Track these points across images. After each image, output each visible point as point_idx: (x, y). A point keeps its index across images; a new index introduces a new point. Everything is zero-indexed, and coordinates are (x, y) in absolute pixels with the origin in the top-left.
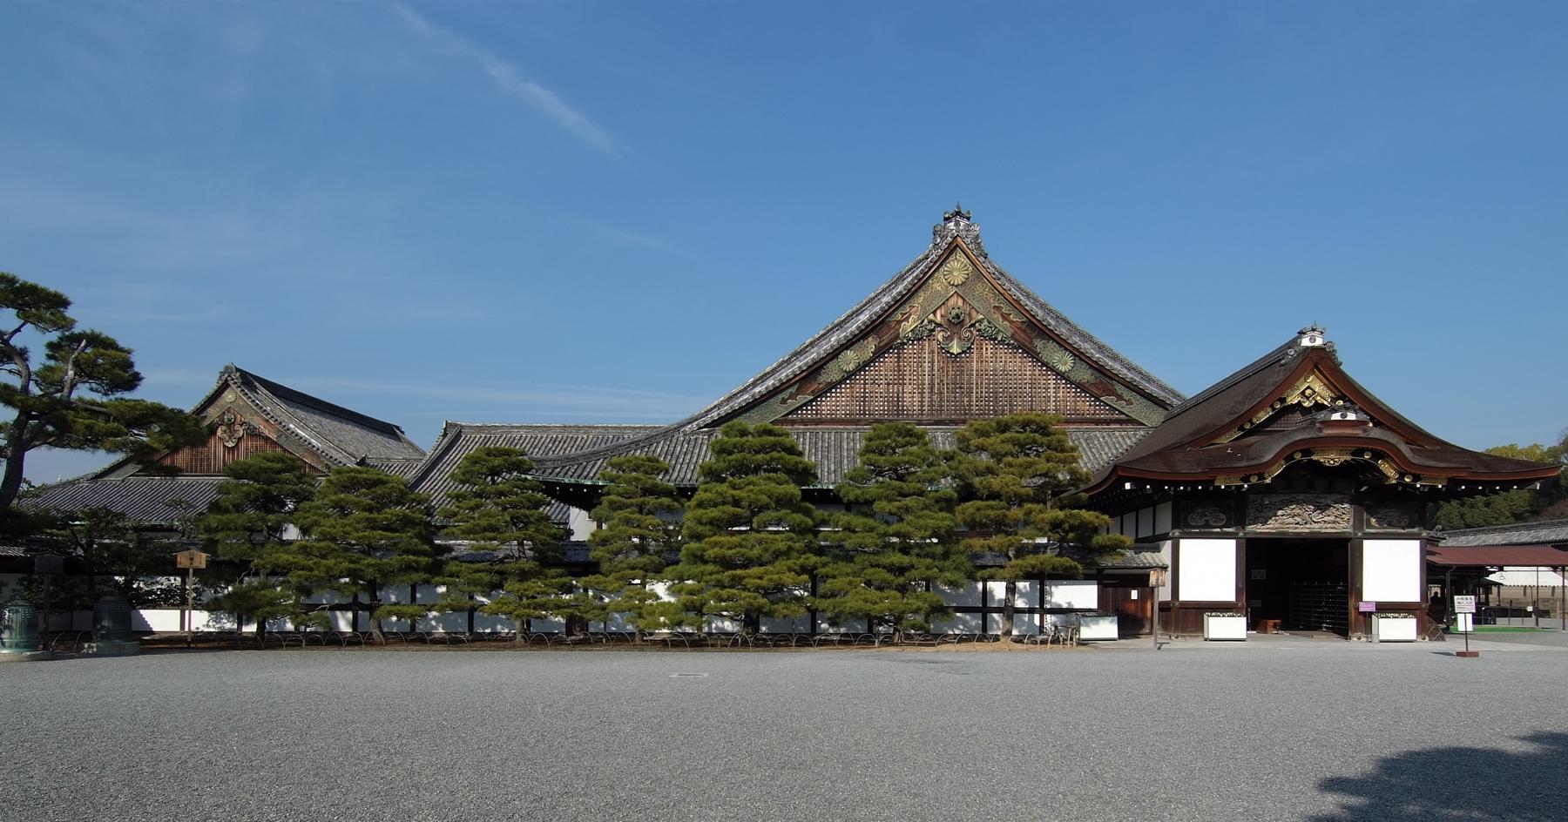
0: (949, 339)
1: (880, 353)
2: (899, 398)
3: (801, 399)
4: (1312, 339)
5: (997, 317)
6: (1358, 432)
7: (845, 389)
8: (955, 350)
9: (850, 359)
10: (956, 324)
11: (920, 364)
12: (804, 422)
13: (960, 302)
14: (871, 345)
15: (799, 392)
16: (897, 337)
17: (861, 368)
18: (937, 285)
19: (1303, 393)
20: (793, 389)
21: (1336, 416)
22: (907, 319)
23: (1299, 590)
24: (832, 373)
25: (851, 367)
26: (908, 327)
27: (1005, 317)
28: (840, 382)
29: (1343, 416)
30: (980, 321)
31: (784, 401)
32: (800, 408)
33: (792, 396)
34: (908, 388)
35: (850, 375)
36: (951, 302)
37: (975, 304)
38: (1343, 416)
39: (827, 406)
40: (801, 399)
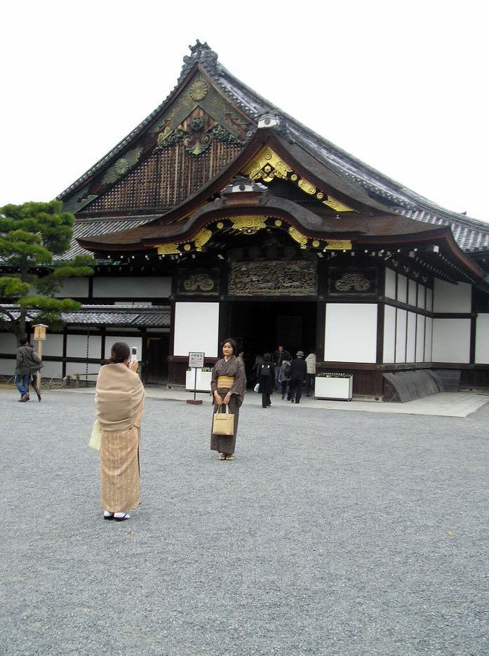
0: (192, 143)
1: (144, 158)
2: (157, 193)
3: (92, 198)
4: (267, 122)
5: (228, 122)
6: (255, 202)
7: (119, 189)
8: (196, 152)
9: (123, 165)
10: (197, 131)
11: (172, 166)
12: (92, 216)
13: (202, 113)
14: (138, 153)
15: (90, 193)
16: (156, 145)
17: (132, 170)
18: (185, 102)
19: (263, 169)
20: (85, 191)
21: (236, 189)
22: (163, 131)
23: (274, 348)
24: (110, 178)
25: (123, 171)
26: (164, 136)
27: (234, 123)
28: (117, 183)
29: (242, 188)
30: (216, 127)
31: (79, 201)
32: (88, 206)
33: (85, 197)
34: (163, 184)
35: (124, 177)
36: (195, 115)
37: (212, 114)
38: (242, 188)
39: (109, 202)
40: (92, 198)
